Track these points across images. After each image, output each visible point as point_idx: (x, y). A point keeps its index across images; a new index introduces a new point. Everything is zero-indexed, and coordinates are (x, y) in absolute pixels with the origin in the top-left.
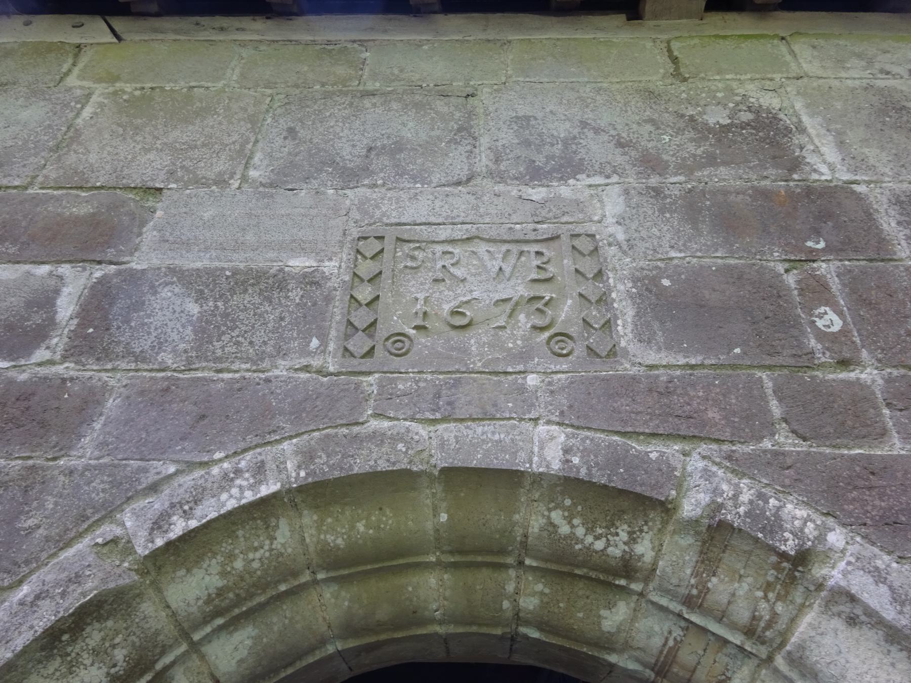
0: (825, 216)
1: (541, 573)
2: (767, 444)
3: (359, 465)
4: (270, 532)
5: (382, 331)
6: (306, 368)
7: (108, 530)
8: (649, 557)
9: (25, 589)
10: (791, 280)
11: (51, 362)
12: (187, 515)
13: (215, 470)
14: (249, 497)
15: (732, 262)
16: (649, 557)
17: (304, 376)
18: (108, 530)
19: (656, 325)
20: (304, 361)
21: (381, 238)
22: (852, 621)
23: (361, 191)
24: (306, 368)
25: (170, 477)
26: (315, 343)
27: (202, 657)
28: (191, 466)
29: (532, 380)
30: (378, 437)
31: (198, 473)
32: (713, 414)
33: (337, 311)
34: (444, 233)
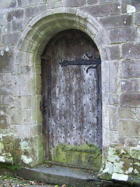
2: (85, 6)
6: (41, 4)
7: (28, 25)
8: (75, 19)
9: (24, 31)
11: (18, 7)
12: (34, 22)
13: (35, 17)
14: (38, 20)
16: (75, 19)
17: (40, 5)
18: (28, 25)
20: (40, 3)
24: (41, 4)
25: (32, 19)
28: (33, 17)
30: (48, 11)
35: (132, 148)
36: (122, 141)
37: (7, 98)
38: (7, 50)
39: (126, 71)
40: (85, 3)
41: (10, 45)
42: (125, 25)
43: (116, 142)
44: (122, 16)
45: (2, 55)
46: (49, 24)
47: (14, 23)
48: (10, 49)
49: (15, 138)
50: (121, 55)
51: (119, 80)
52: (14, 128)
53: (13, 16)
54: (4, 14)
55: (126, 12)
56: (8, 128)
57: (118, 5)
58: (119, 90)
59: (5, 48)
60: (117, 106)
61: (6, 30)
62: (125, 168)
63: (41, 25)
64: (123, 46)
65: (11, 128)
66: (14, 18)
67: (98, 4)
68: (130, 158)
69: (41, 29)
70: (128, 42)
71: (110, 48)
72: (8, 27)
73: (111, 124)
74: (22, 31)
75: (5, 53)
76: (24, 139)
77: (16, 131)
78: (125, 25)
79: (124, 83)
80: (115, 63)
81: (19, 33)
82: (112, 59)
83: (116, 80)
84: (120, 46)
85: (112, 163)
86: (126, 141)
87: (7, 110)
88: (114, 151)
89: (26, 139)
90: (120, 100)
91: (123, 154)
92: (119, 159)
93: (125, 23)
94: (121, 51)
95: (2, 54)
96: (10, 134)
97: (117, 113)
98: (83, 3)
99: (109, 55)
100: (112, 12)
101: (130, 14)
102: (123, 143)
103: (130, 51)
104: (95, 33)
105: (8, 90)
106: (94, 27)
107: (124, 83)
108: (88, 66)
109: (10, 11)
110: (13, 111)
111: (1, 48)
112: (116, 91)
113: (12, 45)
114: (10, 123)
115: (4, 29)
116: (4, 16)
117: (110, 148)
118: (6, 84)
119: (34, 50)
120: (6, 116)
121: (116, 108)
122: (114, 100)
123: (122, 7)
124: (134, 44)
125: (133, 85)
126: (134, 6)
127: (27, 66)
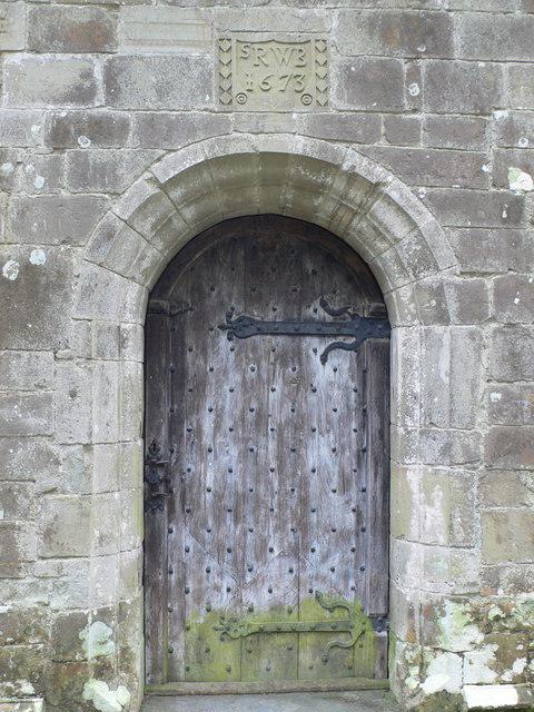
0: (431, 32)
1: (295, 187)
3: (232, 152)
4: (201, 174)
5: (235, 93)
6: (206, 110)
7: (148, 175)
9: (127, 194)
10: (405, 68)
12: (174, 169)
13: (179, 152)
14: (194, 163)
15: (383, 58)
17: (205, 113)
19: (346, 91)
20: (203, 107)
21: (229, 40)
22: (389, 204)
23: (217, 7)
24: (206, 110)
26: (208, 98)
27: (181, 214)
28: (170, 151)
29: (294, 116)
31: (173, 154)
32: (360, 132)
33: (214, 81)
34: (257, 37)
35: (524, 596)
36: (491, 579)
37: (20, 455)
38: (38, 257)
39: (504, 360)
40: (378, 138)
41: (56, 241)
42: (504, 221)
43: (474, 584)
44: (495, 195)
45: (13, 277)
46: (225, 185)
47: (80, 161)
48: (52, 259)
49: (55, 615)
50: (491, 310)
51: (483, 385)
52: (52, 573)
53: (80, 132)
54: (34, 120)
55: (505, 185)
56: (21, 574)
57: (482, 160)
58: (482, 417)
59: (30, 250)
60: (475, 469)
61: (40, 181)
62: (502, 661)
63: (195, 183)
64: (497, 283)
65: (41, 573)
66: (84, 143)
67: (421, 146)
68: (518, 629)
69: (188, 200)
70: (512, 273)
71: (457, 287)
72: (52, 172)
73: (455, 527)
74: (115, 194)
75: (28, 269)
76: (95, 613)
77: (65, 583)
78: (504, 221)
79: (499, 396)
80: (472, 335)
81: (104, 199)
82: (463, 322)
83: (474, 387)
84: (489, 283)
85: (461, 654)
86: (504, 577)
87: (22, 501)
88: (464, 614)
89: (103, 615)
90: (486, 450)
91: (497, 618)
92: (480, 637)
93: (505, 215)
94: (491, 298)
95: (11, 271)
96: (31, 602)
97: (475, 490)
98: (372, 135)
99: (452, 307)
100: (463, 177)
101: (518, 194)
102: (497, 586)
103: (517, 301)
104: (399, 235)
105: (32, 421)
106: (407, 215)
107: (499, 396)
108: (331, 341)
109: (63, 114)
110: (52, 506)
111: (6, 251)
112: (472, 422)
113: (64, 242)
114: (31, 556)
115: (30, 178)
116: (35, 129)
117: (450, 607)
118: (21, 394)
119: (145, 270)
120: (13, 527)
121: (473, 475)
122: (466, 448)
123: (496, 168)
124: (531, 281)
125: (526, 403)
126: (529, 173)
127: (119, 327)
